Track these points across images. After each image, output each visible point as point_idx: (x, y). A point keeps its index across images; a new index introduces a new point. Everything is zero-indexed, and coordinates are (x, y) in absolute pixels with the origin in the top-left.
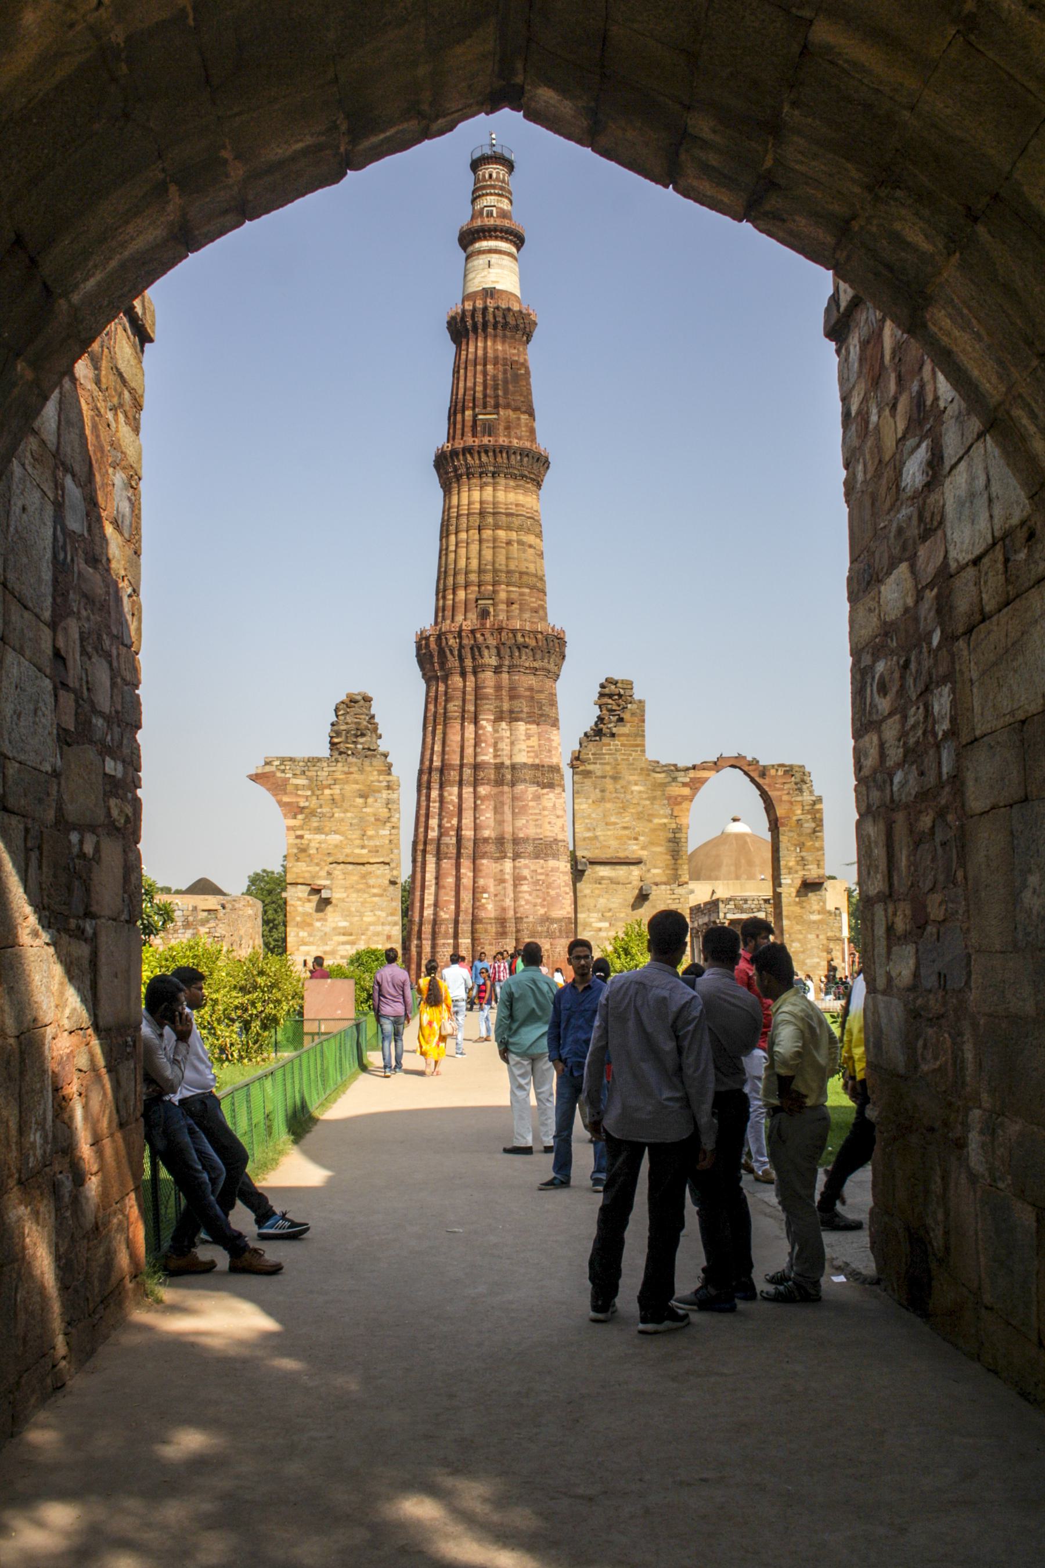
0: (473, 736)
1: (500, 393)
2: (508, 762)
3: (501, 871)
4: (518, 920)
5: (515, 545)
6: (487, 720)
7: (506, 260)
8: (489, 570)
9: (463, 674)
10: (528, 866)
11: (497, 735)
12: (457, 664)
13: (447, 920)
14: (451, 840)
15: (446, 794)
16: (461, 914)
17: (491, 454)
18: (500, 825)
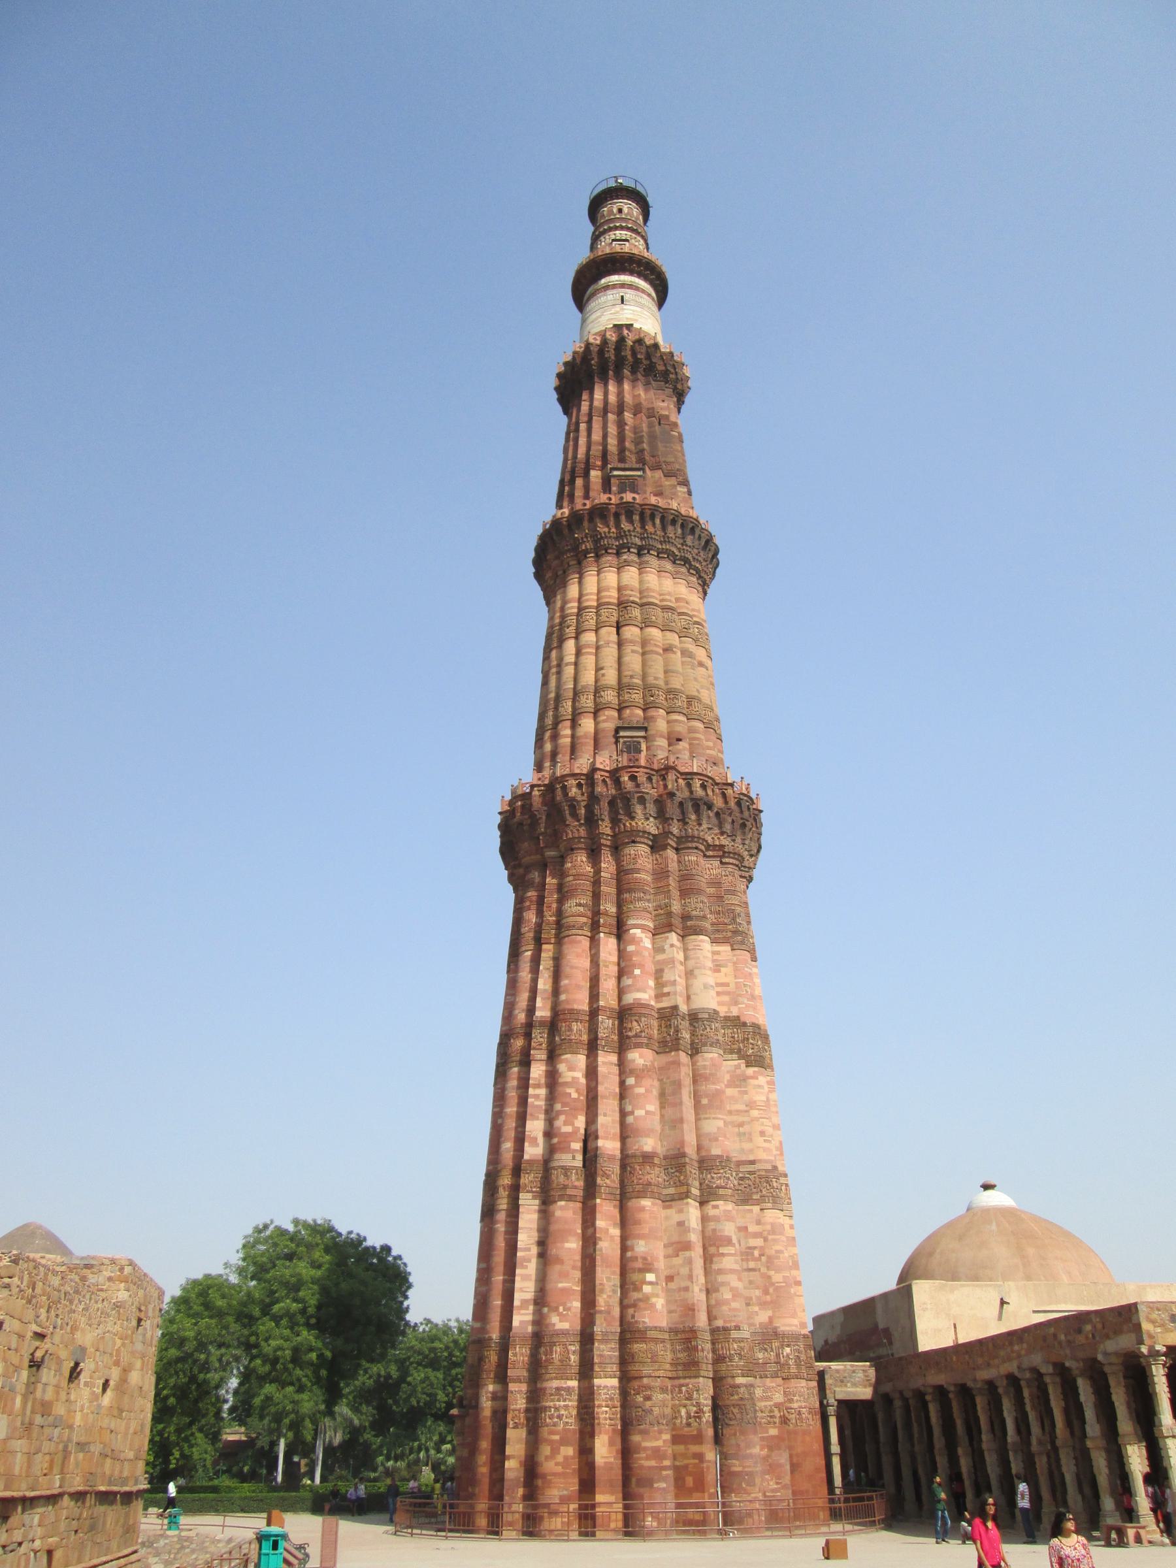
0: (615, 959)
1: (645, 446)
2: (683, 1008)
3: (681, 1224)
4: (719, 1334)
5: (679, 653)
7: (646, 301)
9: (594, 854)
10: (728, 1214)
11: (660, 957)
12: (583, 832)
13: (564, 1333)
15: (562, 1067)
16: (599, 1320)
17: (636, 518)
18: (674, 1127)
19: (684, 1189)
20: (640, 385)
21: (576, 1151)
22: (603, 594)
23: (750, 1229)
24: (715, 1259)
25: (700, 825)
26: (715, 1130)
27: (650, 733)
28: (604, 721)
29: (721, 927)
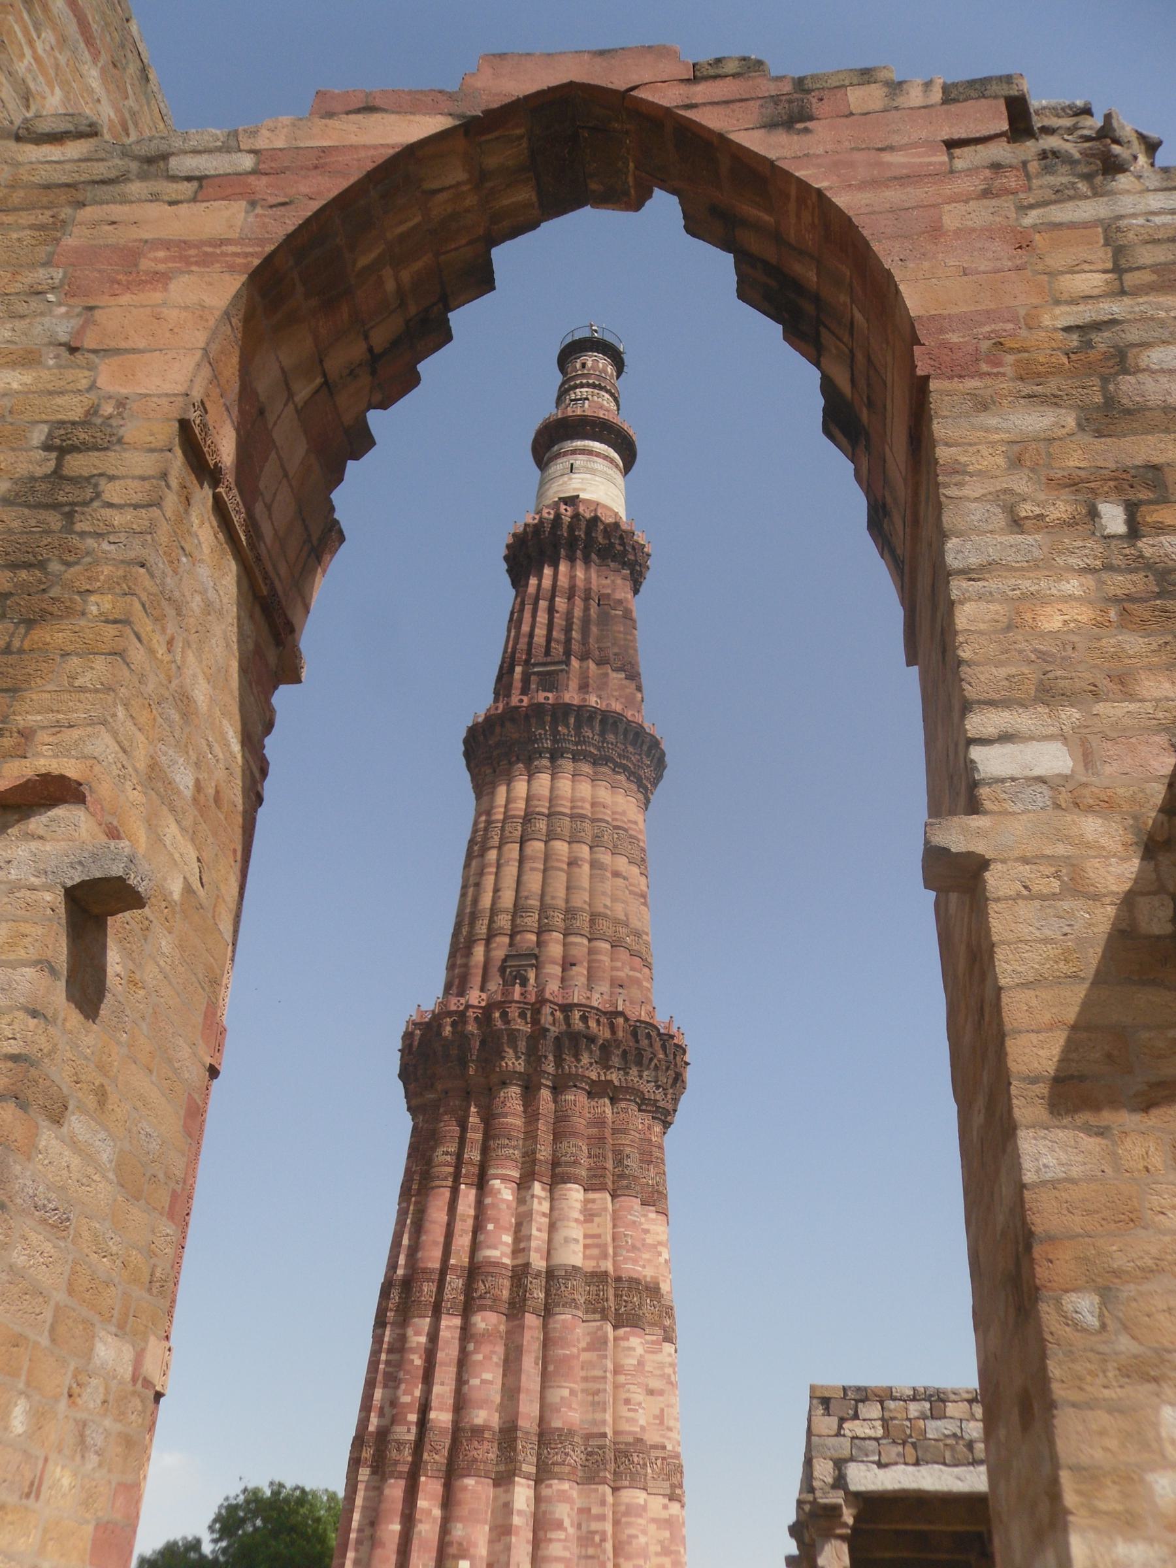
0: (472, 1212)
2: (538, 1262)
5: (586, 867)
6: (504, 1178)
7: (600, 465)
8: (532, 907)
11: (522, 1209)
14: (406, 1433)
15: (410, 1332)
19: (511, 1467)
20: (579, 564)
21: (411, 1423)
22: (512, 806)
23: (594, 1511)
24: (542, 1545)
25: (579, 1061)
26: (558, 1400)
27: (541, 959)
28: (495, 949)
29: (599, 1172)
